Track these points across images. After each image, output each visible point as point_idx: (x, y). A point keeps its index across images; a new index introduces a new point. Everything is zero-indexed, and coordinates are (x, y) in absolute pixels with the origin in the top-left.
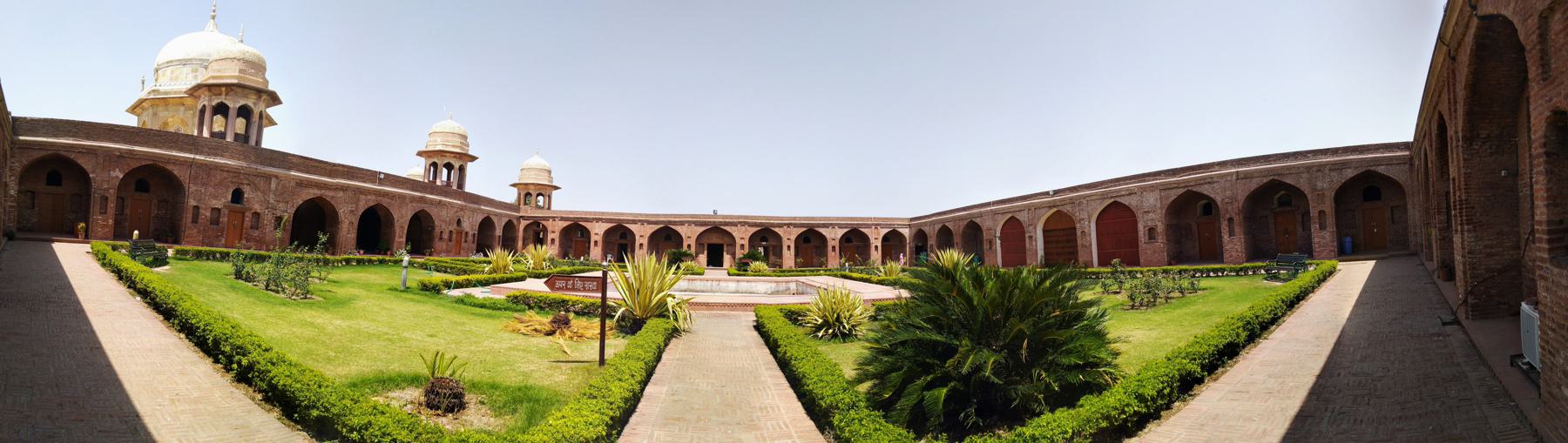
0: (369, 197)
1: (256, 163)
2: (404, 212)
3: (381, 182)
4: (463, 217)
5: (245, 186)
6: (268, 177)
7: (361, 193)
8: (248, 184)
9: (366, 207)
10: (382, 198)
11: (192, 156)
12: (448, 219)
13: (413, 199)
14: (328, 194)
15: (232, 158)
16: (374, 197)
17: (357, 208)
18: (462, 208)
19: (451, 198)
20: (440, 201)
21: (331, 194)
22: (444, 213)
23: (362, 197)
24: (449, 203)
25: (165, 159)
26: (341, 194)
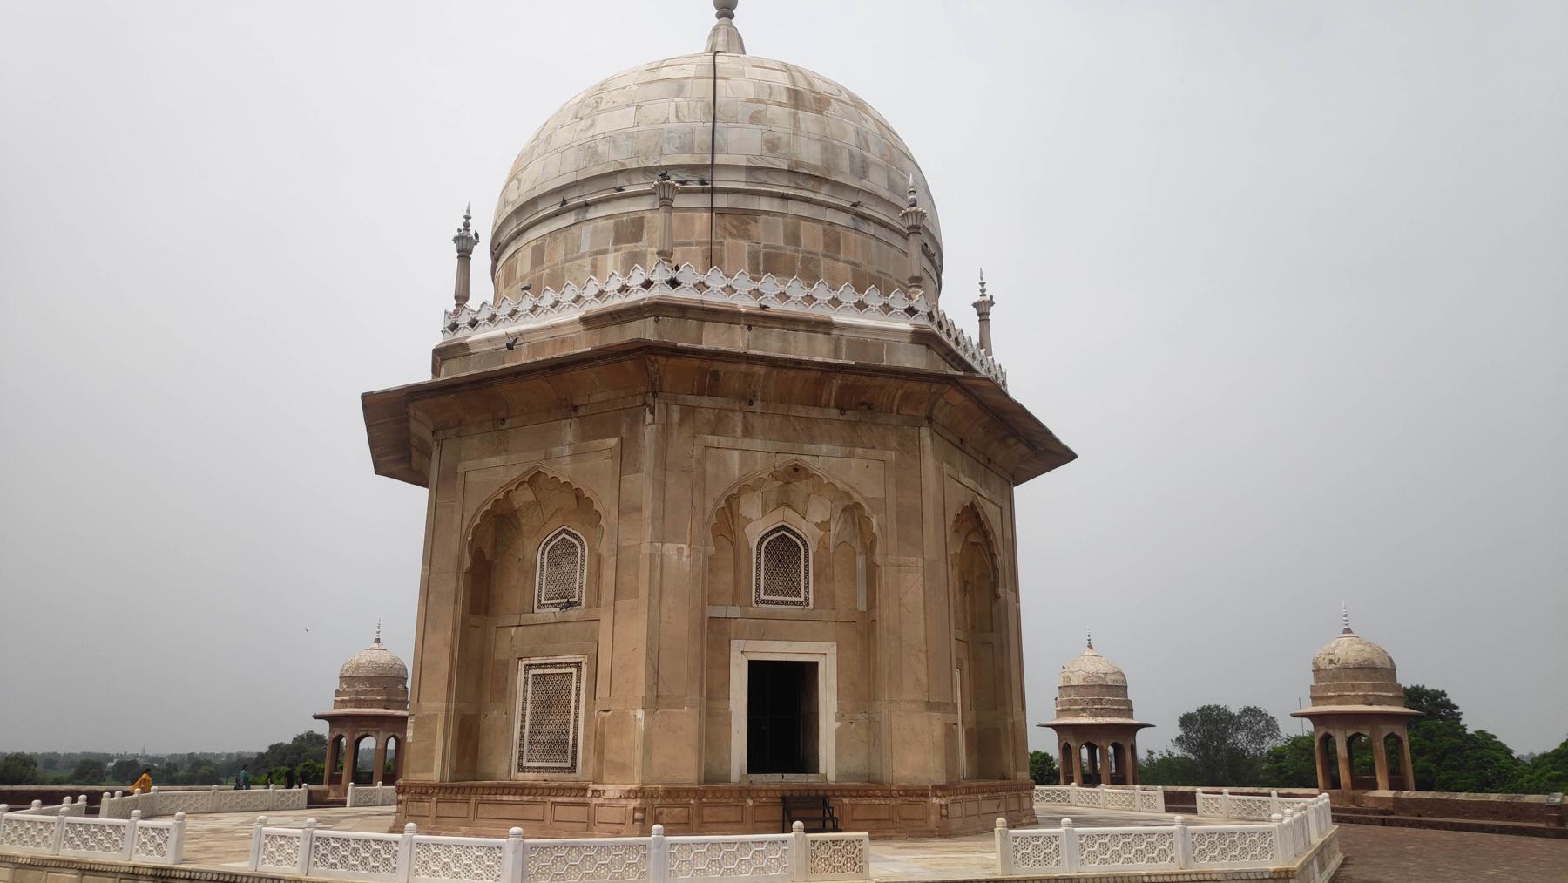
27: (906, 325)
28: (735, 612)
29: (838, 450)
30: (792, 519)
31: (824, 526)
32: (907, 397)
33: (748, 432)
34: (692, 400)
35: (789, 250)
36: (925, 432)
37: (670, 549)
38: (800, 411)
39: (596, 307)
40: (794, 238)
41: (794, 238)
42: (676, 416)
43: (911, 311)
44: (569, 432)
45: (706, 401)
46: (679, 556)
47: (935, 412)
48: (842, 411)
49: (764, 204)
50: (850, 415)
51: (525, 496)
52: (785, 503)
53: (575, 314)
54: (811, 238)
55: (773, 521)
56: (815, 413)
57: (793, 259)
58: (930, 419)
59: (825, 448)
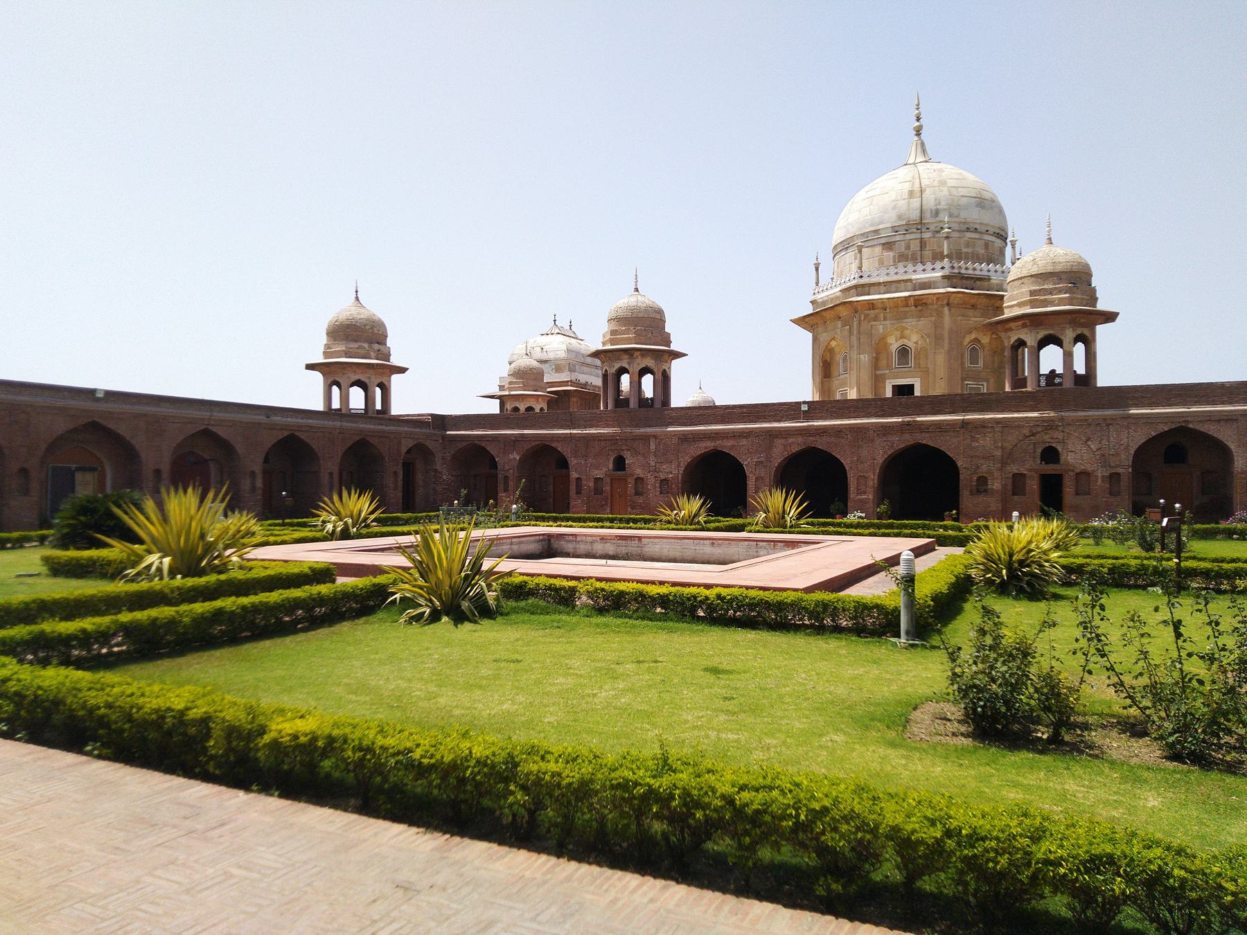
0: (791, 440)
1: (628, 426)
2: (864, 452)
3: (808, 415)
4: (1063, 442)
5: (626, 452)
6: (646, 439)
7: (777, 437)
8: (628, 450)
9: (786, 454)
10: (818, 438)
11: (567, 431)
12: (998, 453)
13: (886, 430)
14: (726, 445)
15: (607, 426)
16: (800, 439)
17: (769, 459)
18: (1049, 425)
19: (1003, 411)
20: (965, 424)
21: (730, 443)
22: (985, 442)
23: (779, 442)
24: (998, 421)
25: (548, 438)
26: (744, 442)
27: (939, 274)
28: (887, 372)
29: (915, 320)
30: (906, 342)
31: (916, 343)
32: (938, 299)
33: (885, 319)
34: (867, 312)
35: (906, 252)
36: (946, 309)
37: (862, 356)
38: (903, 309)
39: (844, 286)
40: (908, 247)
41: (908, 247)
42: (862, 318)
43: (943, 268)
44: (839, 324)
45: (872, 311)
46: (865, 358)
47: (951, 301)
48: (916, 307)
49: (898, 238)
50: (919, 308)
51: (833, 344)
52: (902, 337)
53: (839, 288)
54: (915, 246)
55: (900, 343)
56: (907, 309)
57: (908, 255)
58: (948, 304)
59: (910, 320)
